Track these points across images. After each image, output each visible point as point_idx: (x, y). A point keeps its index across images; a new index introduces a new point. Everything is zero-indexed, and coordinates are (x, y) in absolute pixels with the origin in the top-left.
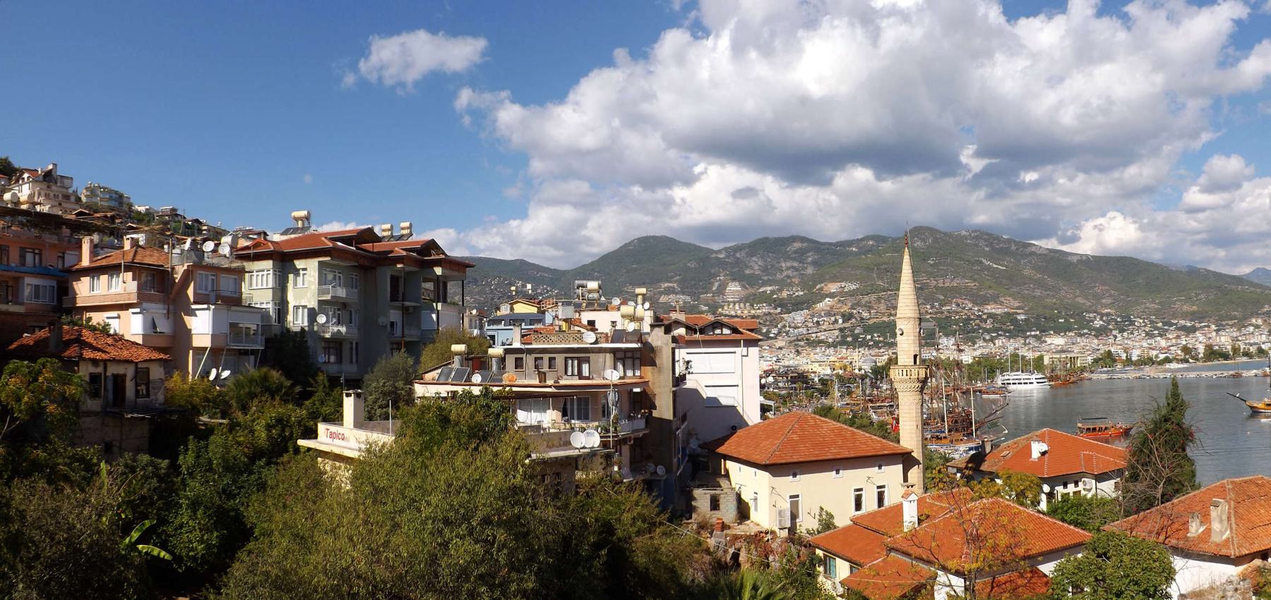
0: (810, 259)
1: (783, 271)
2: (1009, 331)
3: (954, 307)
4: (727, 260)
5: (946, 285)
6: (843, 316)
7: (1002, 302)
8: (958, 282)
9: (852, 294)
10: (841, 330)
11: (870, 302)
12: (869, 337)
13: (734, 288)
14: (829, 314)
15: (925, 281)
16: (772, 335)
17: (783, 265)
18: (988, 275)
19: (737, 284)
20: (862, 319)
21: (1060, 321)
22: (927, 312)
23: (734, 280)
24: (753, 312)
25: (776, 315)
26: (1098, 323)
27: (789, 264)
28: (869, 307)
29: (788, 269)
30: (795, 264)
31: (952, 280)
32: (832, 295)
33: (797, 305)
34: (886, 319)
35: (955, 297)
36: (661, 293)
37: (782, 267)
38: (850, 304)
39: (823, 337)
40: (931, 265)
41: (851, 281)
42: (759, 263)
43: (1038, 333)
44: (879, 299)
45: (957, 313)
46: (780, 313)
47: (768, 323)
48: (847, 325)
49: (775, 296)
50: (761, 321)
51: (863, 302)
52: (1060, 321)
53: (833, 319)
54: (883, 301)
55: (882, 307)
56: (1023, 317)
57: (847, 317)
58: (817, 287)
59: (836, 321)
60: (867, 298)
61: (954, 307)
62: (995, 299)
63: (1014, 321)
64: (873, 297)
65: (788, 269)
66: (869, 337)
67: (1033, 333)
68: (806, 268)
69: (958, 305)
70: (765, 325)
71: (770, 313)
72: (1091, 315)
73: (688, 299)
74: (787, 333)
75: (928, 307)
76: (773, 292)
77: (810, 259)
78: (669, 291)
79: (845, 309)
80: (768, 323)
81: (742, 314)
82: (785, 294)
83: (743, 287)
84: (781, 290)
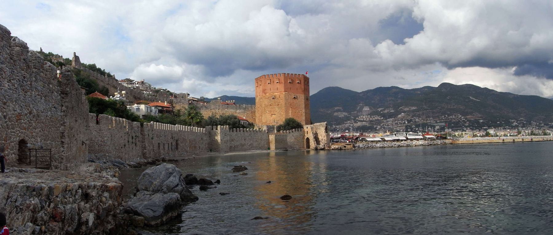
0: (399, 96)
1: (388, 101)
2: (475, 127)
3: (454, 117)
4: (363, 97)
5: (452, 107)
6: (408, 121)
7: (474, 115)
8: (456, 106)
9: (413, 111)
10: (406, 126)
11: (419, 115)
12: (417, 129)
13: (366, 109)
14: (402, 120)
15: (443, 106)
16: (377, 129)
17: (388, 99)
18: (472, 104)
19: (368, 107)
20: (415, 122)
21: (498, 123)
22: (442, 119)
23: (366, 105)
24: (371, 119)
25: (381, 120)
26: (515, 124)
27: (390, 99)
28: (419, 116)
29: (390, 100)
30: (393, 99)
31: (454, 105)
32: (404, 112)
33: (391, 116)
34: (425, 122)
35: (455, 113)
36: (335, 112)
37: (387, 100)
38: (411, 116)
39: (398, 129)
40: (448, 99)
41: (412, 106)
42: (378, 98)
43: (487, 127)
44: (423, 113)
45: (454, 119)
46: (382, 120)
47: (377, 124)
48: (409, 124)
49: (382, 112)
50: (374, 123)
51: (417, 114)
52: (498, 123)
53: (404, 122)
54: (425, 114)
55: (424, 117)
56: (482, 121)
57: (409, 121)
58: (400, 108)
59: (405, 122)
60: (418, 113)
61: (454, 117)
62: (471, 113)
63: (478, 123)
64: (421, 113)
65: (390, 100)
66: (417, 129)
67: (485, 128)
68: (398, 100)
69: (455, 116)
70: (375, 125)
71: (378, 120)
72: (513, 121)
73: (346, 114)
74: (384, 128)
75: (443, 117)
76: (381, 111)
77: (399, 96)
78: (338, 111)
79: (409, 118)
80: (377, 124)
81: (366, 120)
82: (386, 111)
83: (370, 108)
84: (384, 110)
